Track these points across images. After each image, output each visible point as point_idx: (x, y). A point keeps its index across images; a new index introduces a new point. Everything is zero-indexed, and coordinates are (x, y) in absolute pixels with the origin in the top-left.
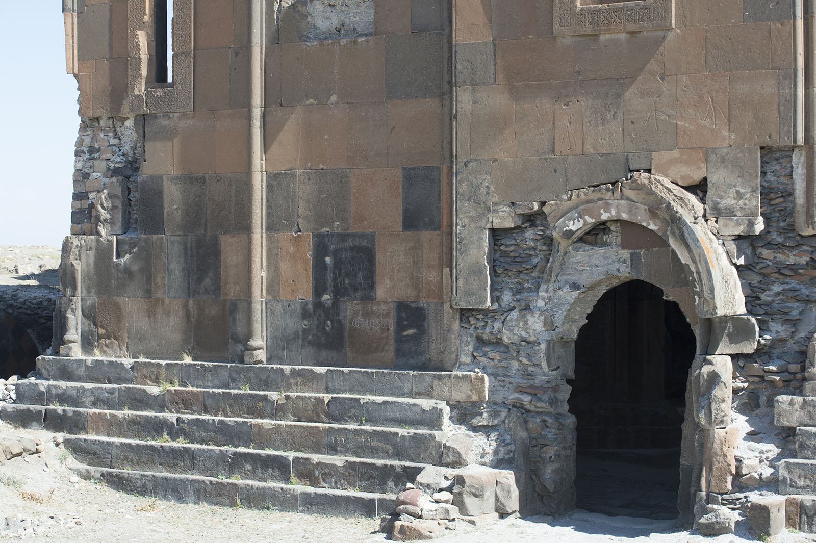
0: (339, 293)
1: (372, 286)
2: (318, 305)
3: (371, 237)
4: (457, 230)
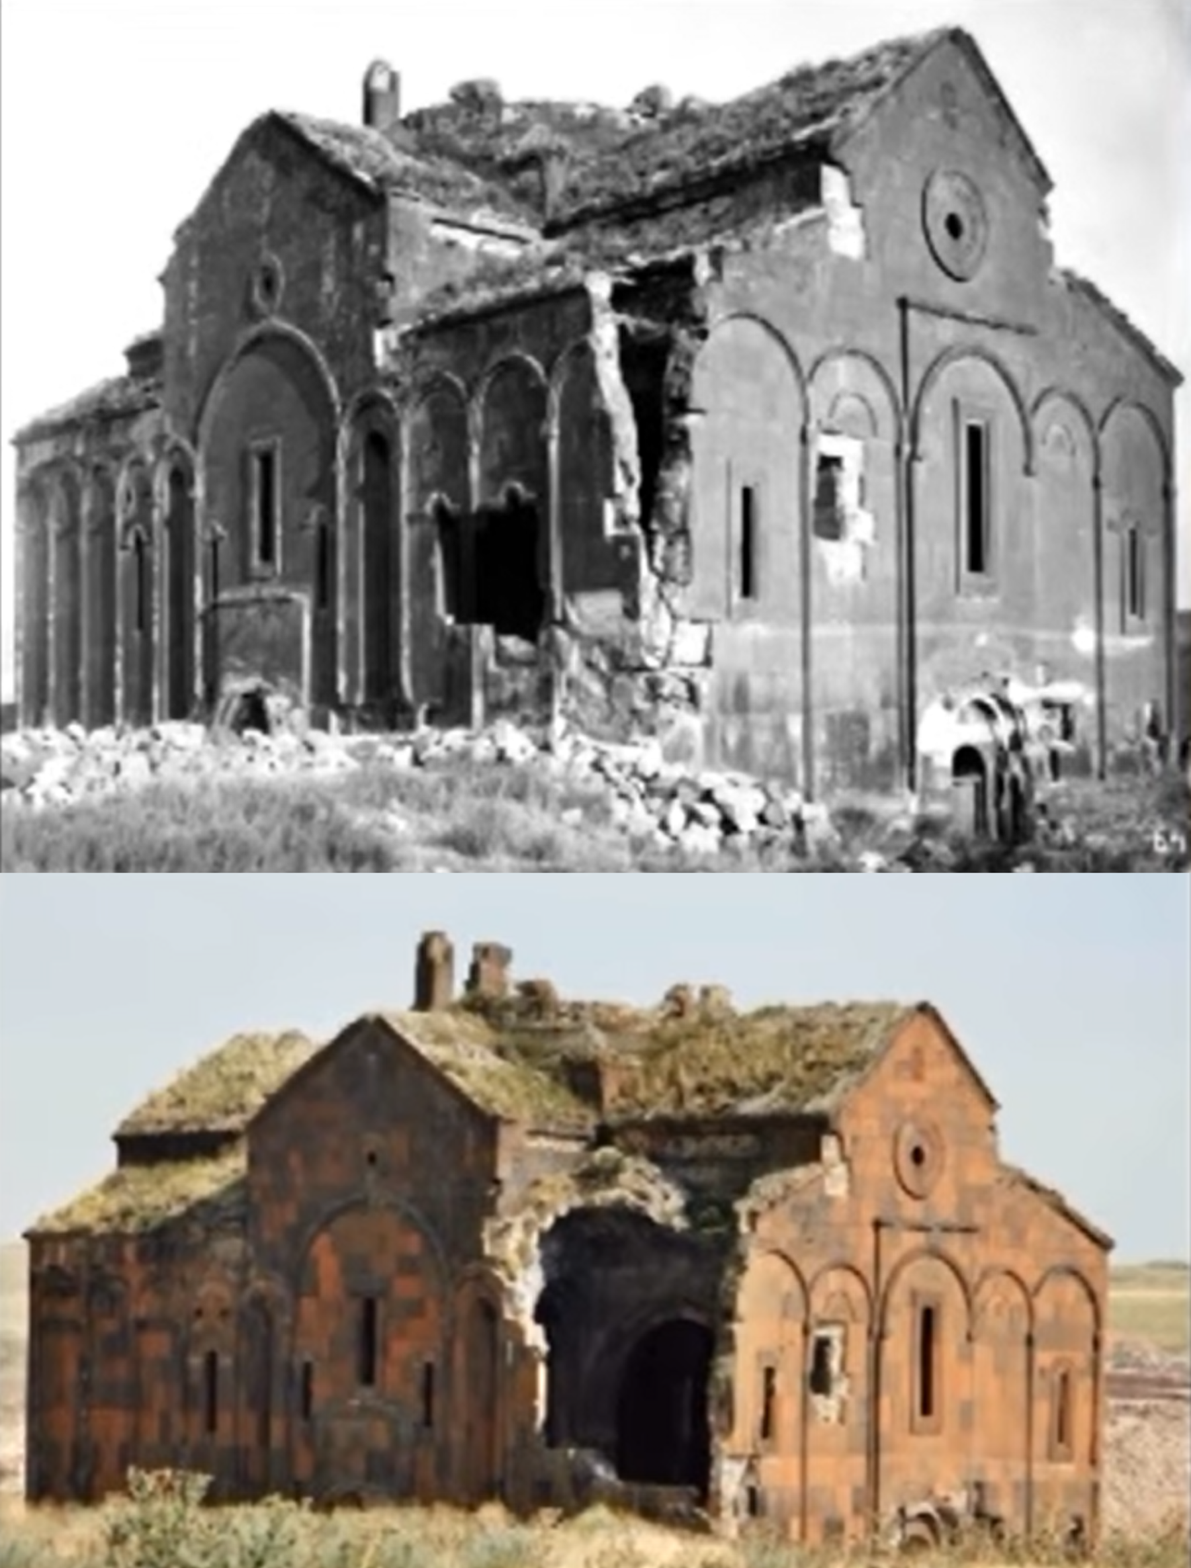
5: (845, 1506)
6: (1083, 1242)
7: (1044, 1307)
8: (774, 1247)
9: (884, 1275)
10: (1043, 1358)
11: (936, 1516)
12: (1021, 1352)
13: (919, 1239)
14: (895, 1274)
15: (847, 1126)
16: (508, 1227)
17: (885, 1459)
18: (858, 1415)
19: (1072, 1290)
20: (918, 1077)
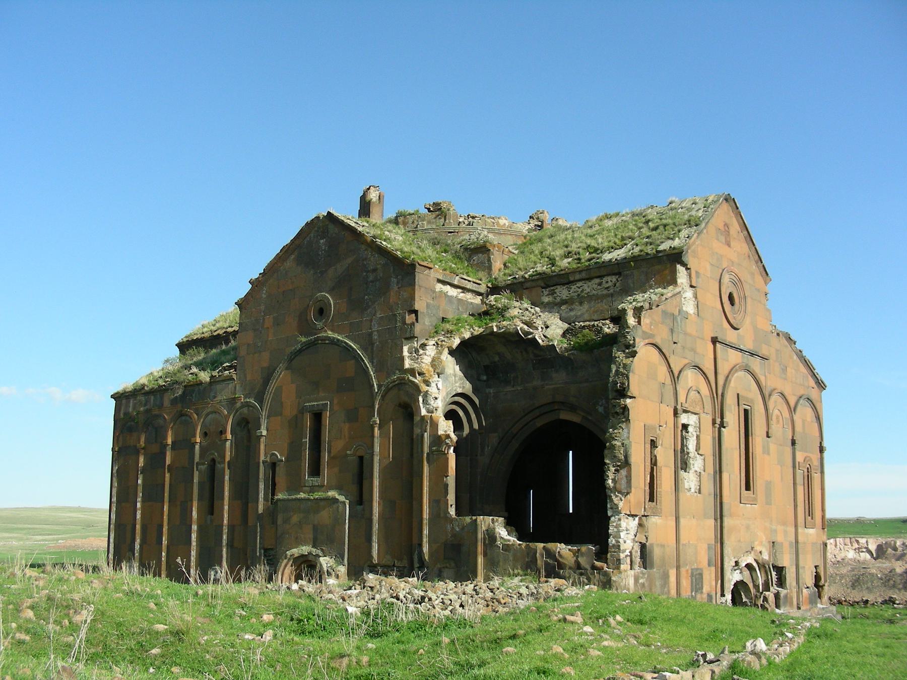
0: (696, 592)
1: (702, 588)
3: (701, 569)
6: (812, 383)
8: (651, 341)
11: (755, 564)
16: (423, 346)
17: (727, 522)
18: (708, 487)
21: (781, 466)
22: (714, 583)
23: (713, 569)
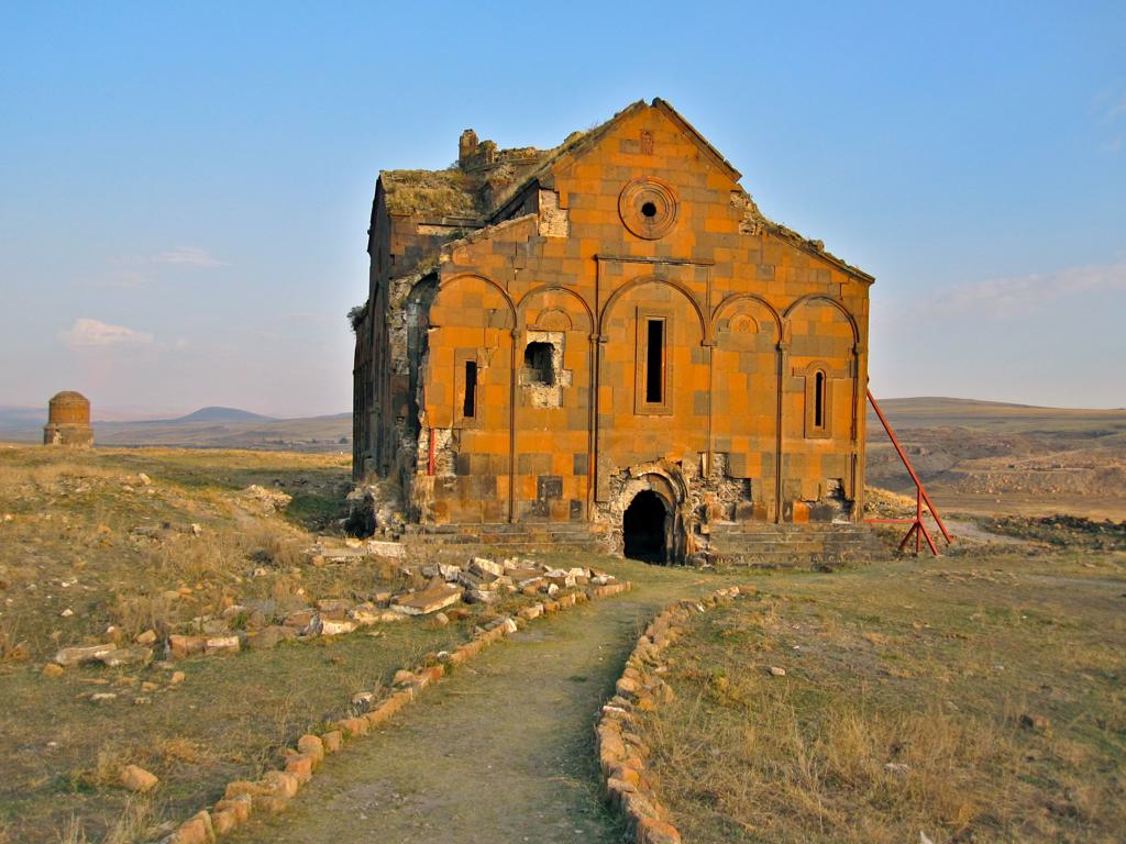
0: (548, 497)
2: (539, 501)
3: (562, 477)
4: (599, 476)
5: (565, 467)
6: (839, 277)
7: (796, 323)
9: (603, 297)
10: (791, 362)
11: (665, 475)
12: (773, 356)
13: (649, 269)
14: (614, 295)
15: (560, 185)
19: (828, 313)
20: (650, 154)
21: (748, 374)
22: (585, 491)
23: (584, 479)
